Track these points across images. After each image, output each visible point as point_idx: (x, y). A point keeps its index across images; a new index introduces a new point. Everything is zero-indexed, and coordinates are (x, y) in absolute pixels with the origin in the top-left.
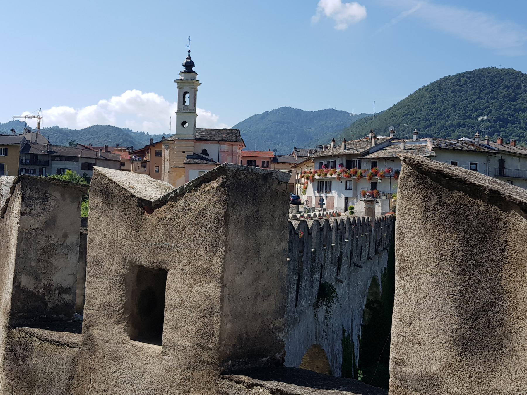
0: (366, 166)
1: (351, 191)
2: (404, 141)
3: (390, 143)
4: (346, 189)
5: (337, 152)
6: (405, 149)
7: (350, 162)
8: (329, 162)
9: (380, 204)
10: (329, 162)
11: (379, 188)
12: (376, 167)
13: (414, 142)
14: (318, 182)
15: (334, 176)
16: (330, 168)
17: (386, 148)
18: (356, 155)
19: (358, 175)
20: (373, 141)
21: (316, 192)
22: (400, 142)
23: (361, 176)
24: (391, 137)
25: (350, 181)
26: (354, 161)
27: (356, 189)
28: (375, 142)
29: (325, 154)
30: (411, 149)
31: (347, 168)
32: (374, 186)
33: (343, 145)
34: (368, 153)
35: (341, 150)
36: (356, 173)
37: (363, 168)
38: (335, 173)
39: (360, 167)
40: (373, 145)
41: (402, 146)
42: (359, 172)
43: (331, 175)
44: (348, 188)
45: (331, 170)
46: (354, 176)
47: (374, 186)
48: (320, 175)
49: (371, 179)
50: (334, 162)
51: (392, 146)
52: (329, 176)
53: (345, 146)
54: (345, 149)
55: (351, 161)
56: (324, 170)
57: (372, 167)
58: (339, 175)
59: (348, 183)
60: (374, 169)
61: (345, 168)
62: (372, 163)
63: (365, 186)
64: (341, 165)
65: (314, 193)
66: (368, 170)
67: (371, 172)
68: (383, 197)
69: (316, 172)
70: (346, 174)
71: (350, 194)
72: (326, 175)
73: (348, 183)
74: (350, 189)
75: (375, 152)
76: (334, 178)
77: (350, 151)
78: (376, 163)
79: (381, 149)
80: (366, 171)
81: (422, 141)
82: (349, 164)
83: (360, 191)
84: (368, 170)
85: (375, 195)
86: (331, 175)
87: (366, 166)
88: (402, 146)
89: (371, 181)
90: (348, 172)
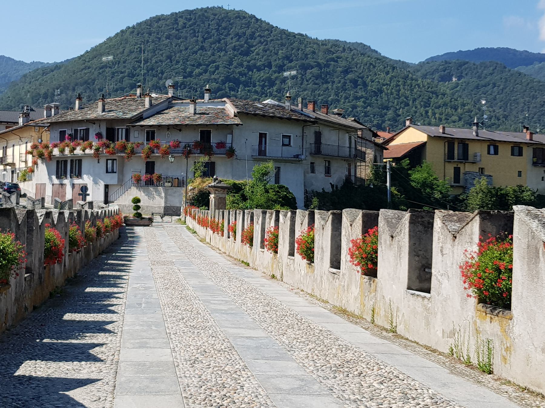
0: (137, 138)
1: (115, 176)
2: (194, 101)
3: (169, 105)
4: (107, 172)
5: (92, 115)
7: (111, 130)
8: (76, 131)
9: (163, 195)
10: (76, 131)
11: (158, 171)
12: (153, 138)
13: (206, 104)
15: (88, 151)
17: (166, 111)
18: (122, 121)
19: (128, 151)
20: (147, 100)
22: (186, 103)
23: (133, 152)
24: (170, 95)
25: (113, 160)
26: (118, 129)
27: (122, 173)
28: (150, 101)
29: (69, 118)
31: (107, 138)
32: (150, 167)
33: (100, 104)
34: (140, 118)
35: (97, 112)
38: (91, 147)
39: (127, 139)
40: (147, 105)
43: (84, 151)
44: (110, 170)
47: (150, 167)
48: (62, 151)
49: (148, 157)
50: (87, 130)
51: (176, 108)
52: (78, 151)
53: (104, 106)
54: (104, 110)
55: (113, 130)
57: (148, 140)
58: (97, 150)
59: (110, 162)
60: (152, 143)
61: (104, 140)
62: (148, 133)
63: (137, 167)
64: (99, 136)
66: (143, 144)
67: (147, 146)
68: (166, 184)
69: (55, 146)
70: (108, 149)
71: (113, 179)
72: (74, 149)
73: (110, 162)
74: (113, 172)
75: (151, 116)
76: (89, 156)
77: (112, 114)
78: (153, 133)
79: (159, 113)
80: (138, 145)
81: (218, 102)
82: (111, 135)
83: (129, 175)
85: (155, 181)
86: (84, 151)
87: (137, 138)
89: (148, 160)
90: (112, 146)
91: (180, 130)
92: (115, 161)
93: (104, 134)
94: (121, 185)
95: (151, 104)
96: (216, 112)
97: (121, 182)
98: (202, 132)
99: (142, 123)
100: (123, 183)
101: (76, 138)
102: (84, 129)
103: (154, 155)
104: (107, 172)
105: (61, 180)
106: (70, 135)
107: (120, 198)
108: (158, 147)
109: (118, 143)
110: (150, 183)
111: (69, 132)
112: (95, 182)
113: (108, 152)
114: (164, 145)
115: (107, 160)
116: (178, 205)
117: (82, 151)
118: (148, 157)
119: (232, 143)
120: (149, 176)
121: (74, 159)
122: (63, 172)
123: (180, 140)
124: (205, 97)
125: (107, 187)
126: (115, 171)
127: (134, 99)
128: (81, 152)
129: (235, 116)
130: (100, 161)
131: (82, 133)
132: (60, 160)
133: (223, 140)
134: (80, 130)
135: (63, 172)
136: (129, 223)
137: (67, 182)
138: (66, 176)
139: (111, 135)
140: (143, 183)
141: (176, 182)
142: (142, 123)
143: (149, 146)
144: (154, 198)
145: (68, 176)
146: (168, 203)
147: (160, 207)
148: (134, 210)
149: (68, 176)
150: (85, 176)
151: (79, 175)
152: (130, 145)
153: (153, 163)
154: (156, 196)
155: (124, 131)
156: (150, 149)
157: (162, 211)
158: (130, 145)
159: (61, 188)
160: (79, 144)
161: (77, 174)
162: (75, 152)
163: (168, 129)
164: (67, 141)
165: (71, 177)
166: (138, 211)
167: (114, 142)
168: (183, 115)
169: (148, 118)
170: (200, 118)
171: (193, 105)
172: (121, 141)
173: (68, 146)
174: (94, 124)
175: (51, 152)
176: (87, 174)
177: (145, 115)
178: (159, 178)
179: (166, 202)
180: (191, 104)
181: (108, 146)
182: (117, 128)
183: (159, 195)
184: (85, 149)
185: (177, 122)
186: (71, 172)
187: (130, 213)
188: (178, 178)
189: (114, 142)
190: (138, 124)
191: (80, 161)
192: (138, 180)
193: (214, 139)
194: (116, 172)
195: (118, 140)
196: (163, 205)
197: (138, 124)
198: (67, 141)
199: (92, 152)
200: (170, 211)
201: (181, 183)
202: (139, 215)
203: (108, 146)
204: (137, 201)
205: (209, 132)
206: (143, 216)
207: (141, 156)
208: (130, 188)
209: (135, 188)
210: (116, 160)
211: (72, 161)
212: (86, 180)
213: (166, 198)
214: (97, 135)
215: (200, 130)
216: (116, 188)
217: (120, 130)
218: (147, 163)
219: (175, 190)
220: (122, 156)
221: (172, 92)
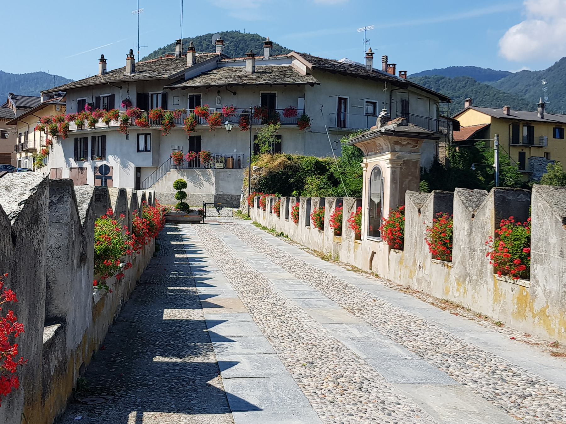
0: (178, 104)
1: (149, 155)
4: (138, 151)
6: (253, 72)
9: (213, 180)
10: (98, 99)
11: (206, 147)
12: (198, 104)
14: (76, 140)
15: (113, 123)
16: (101, 111)
18: (158, 82)
19: (166, 121)
21: (72, 160)
23: (172, 123)
25: (146, 135)
26: (152, 95)
30: (265, 72)
31: (138, 105)
32: (195, 143)
34: (181, 78)
36: (160, 117)
37: (171, 107)
38: (116, 118)
39: (164, 106)
40: (190, 63)
41: (249, 66)
42: (167, 114)
43: (107, 123)
44: (142, 147)
45: (107, 115)
46: (159, 123)
47: (195, 143)
48: (80, 125)
50: (112, 98)
52: (101, 124)
56: (93, 115)
57: (191, 107)
58: (125, 121)
59: (142, 138)
60: (197, 110)
61: (134, 108)
62: (191, 98)
63: (177, 143)
64: (127, 103)
65: (68, 162)
66: (185, 112)
67: (190, 116)
68: (217, 165)
69: (72, 118)
70: (139, 120)
71: (146, 160)
72: (96, 121)
73: (142, 138)
74: (146, 150)
75: (196, 77)
77: (144, 74)
78: (198, 98)
82: (143, 102)
83: (167, 154)
84: (185, 112)
86: (107, 123)
87: (178, 104)
88: (249, 66)
89: (193, 134)
90: (144, 115)
91: (235, 94)
92: (148, 137)
93: (134, 100)
94: (157, 168)
95: (194, 62)
96: (280, 70)
97: (157, 164)
98: (264, 96)
99: (184, 84)
100: (160, 165)
101: (98, 107)
102: (107, 97)
103: (200, 126)
104: (138, 151)
105: (80, 163)
106: (90, 104)
107: (156, 185)
108: (205, 115)
109: (153, 112)
110: (194, 164)
111: (89, 100)
112: (124, 165)
113: (140, 123)
114: (214, 113)
115: (138, 135)
116: (233, 192)
117: (105, 123)
118: (192, 129)
119: (304, 110)
120: (194, 154)
121: (96, 135)
122: (82, 153)
123: (234, 106)
124: (265, 53)
125: (138, 170)
126: (148, 149)
127: (171, 59)
128: (104, 125)
129: (307, 74)
130: (130, 137)
131: (105, 102)
132: (79, 137)
133: (293, 106)
134: (104, 97)
135: (82, 153)
136: (170, 218)
137: (87, 165)
138: (86, 158)
139: (143, 102)
140: (185, 164)
141: (231, 163)
142: (184, 84)
143: (194, 114)
144: (201, 185)
145: (89, 158)
146: (220, 190)
147: (209, 196)
148: (178, 199)
149: (89, 158)
150: (110, 157)
151: (103, 156)
152: (168, 114)
153: (199, 138)
154: (204, 182)
155: (160, 97)
156: (195, 118)
157: (212, 201)
158: (168, 113)
159: (80, 174)
160: (101, 116)
161: (100, 155)
162: (97, 125)
163: (219, 92)
164: (87, 112)
165: (92, 159)
166: (183, 201)
167: (146, 110)
168: (237, 74)
169: (192, 79)
170: (261, 77)
171: (250, 61)
172: (156, 109)
173: (87, 118)
174: (121, 88)
175: (67, 127)
176: (113, 154)
177: (187, 75)
178: (208, 157)
179: (217, 189)
180: (248, 59)
181: (139, 116)
182: (150, 93)
183: (208, 180)
184: (110, 121)
185: (230, 81)
186: (93, 153)
187: (170, 203)
188: (232, 157)
189: (146, 110)
190: (178, 85)
191: (104, 138)
192: (179, 160)
193: (280, 105)
194: (150, 151)
195: (152, 108)
196: (214, 193)
197: (178, 85)
198: (87, 112)
199: (118, 124)
200: (224, 201)
201: (237, 165)
202: (184, 207)
203: (139, 116)
204: (181, 185)
205: (273, 96)
206: (191, 208)
207: (183, 130)
208: (169, 171)
209: (176, 172)
210: (150, 134)
211: (93, 138)
212: (112, 161)
213: (217, 183)
214: (123, 102)
215: (261, 92)
216: (149, 172)
217: (155, 96)
218: (191, 139)
219: (229, 173)
220: (159, 131)
221: (220, 49)
